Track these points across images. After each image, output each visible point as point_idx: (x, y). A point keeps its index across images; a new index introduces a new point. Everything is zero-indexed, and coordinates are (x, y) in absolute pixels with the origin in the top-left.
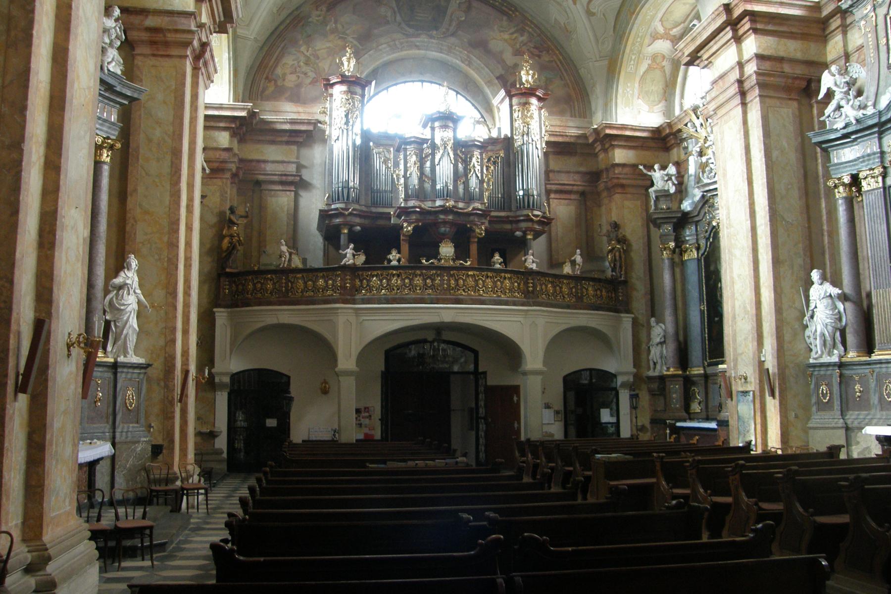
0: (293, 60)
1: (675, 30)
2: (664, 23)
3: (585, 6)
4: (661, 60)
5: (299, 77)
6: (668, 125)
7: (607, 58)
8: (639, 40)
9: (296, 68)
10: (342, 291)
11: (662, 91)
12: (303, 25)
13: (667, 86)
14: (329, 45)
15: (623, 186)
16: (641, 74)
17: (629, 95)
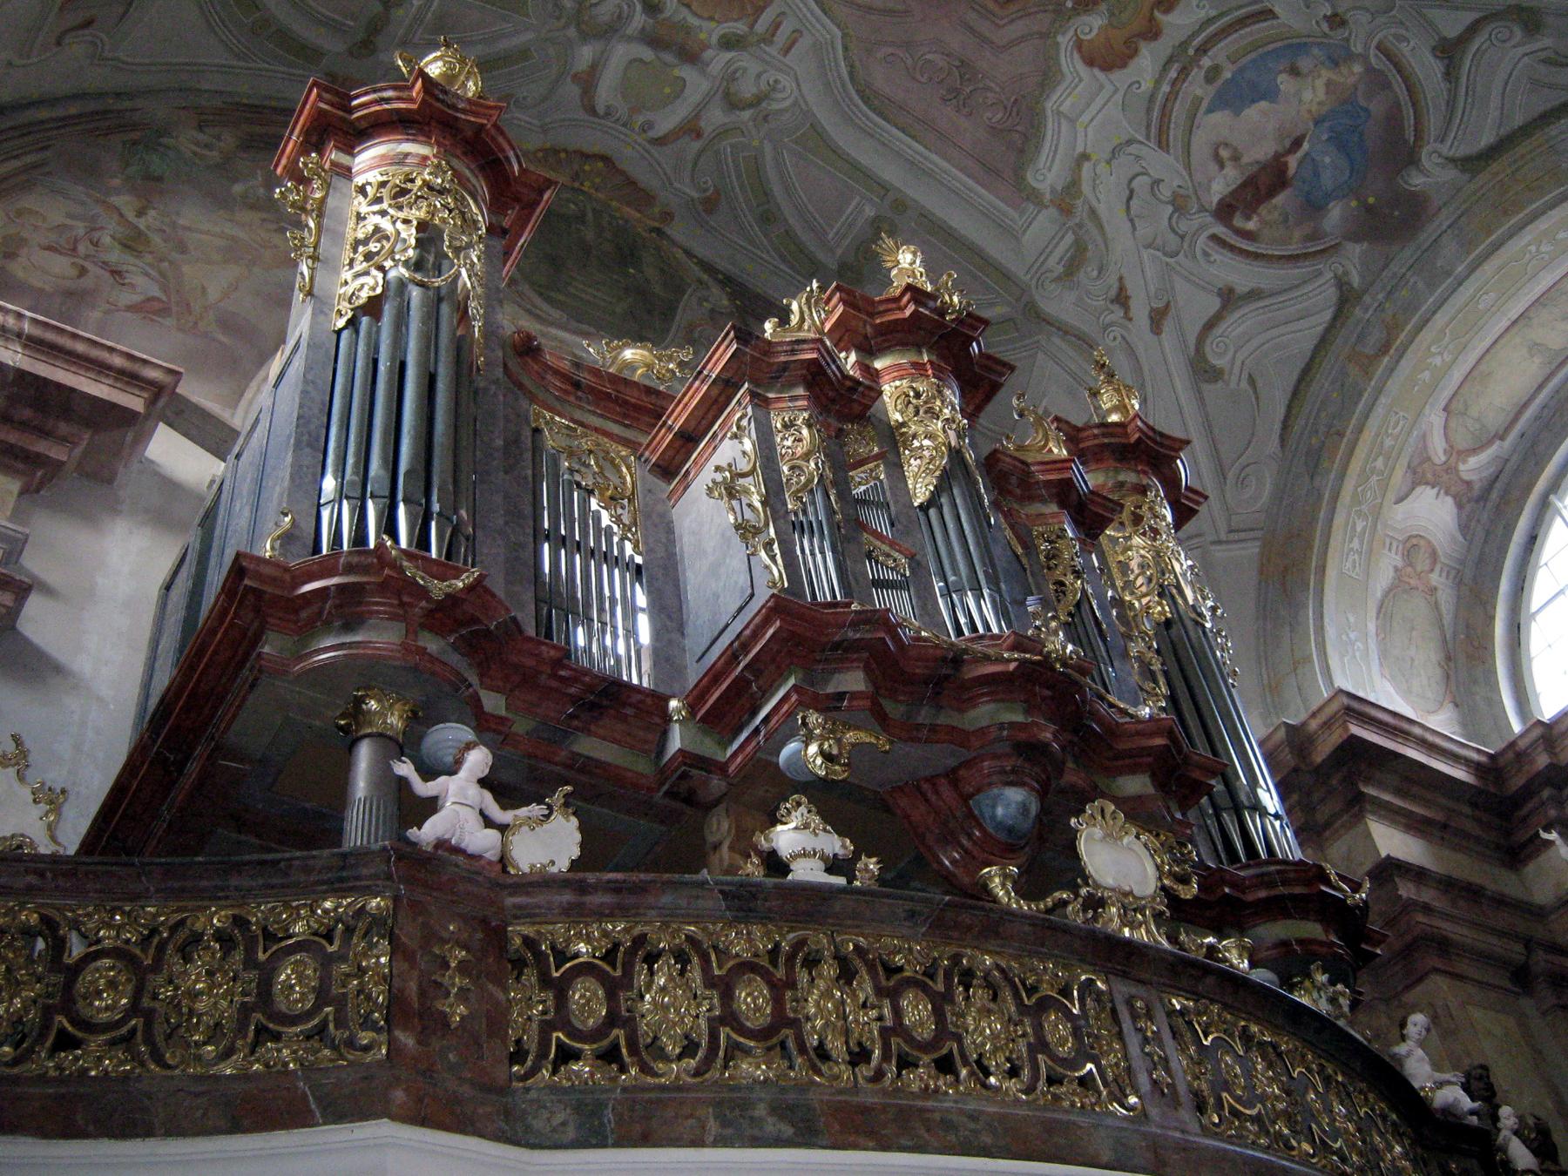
0: (69, 216)
1: (1473, 461)
2: (1453, 424)
3: (1192, 341)
4: (1427, 568)
5: (83, 271)
6: (1542, 737)
7: (1258, 534)
8: (1380, 463)
9: (76, 241)
10: (407, 1039)
11: (1439, 671)
12: (135, 143)
13: (1449, 658)
14: (230, 230)
15: (1443, 945)
16: (1379, 594)
17: (1357, 654)
